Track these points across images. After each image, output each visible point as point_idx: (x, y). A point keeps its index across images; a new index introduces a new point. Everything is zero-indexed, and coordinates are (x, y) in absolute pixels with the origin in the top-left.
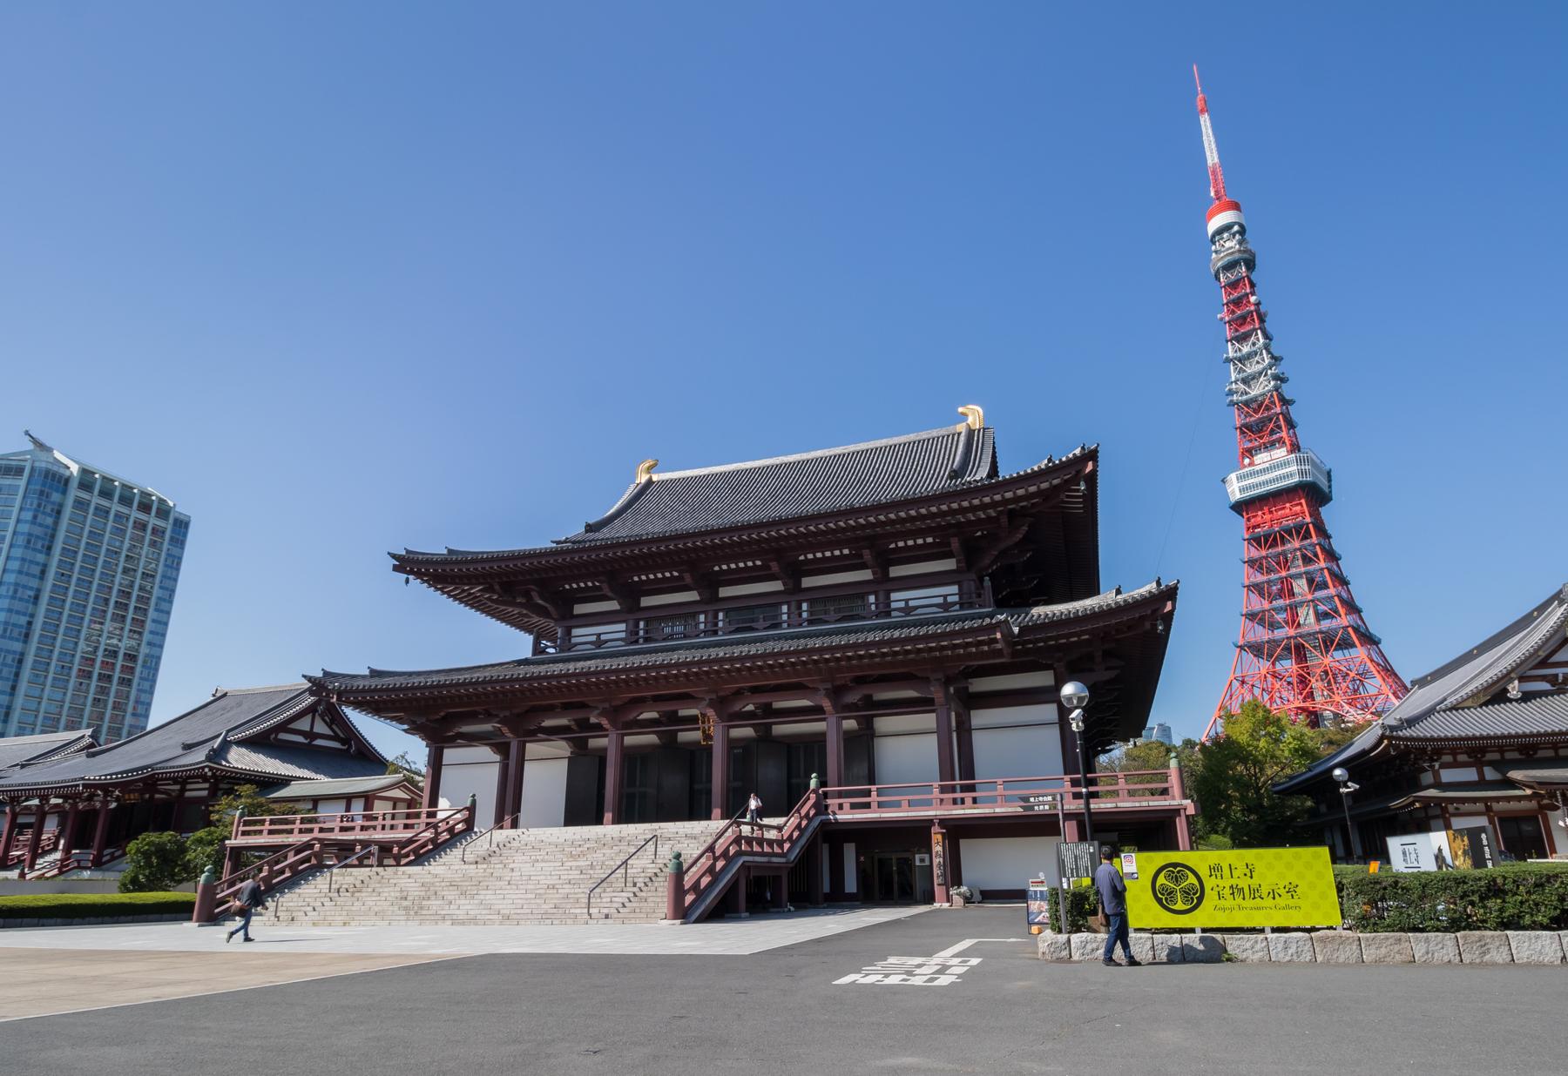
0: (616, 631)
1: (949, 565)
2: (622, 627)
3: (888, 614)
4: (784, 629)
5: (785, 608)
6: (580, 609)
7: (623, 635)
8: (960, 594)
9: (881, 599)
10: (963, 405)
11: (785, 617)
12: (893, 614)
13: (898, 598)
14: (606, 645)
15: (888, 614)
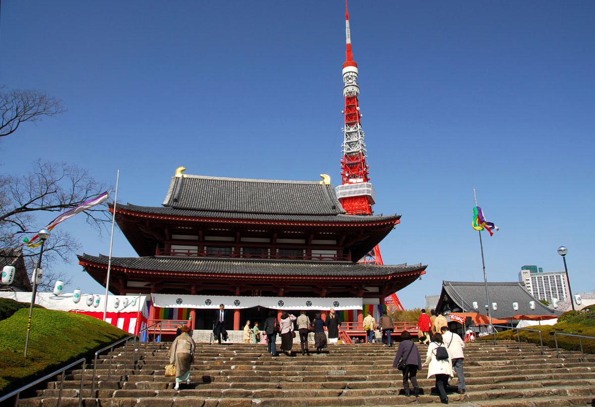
0: (194, 249)
1: (333, 242)
2: (196, 248)
3: (310, 259)
6: (175, 237)
11: (269, 254)
12: (313, 259)
13: (315, 253)
15: (310, 259)
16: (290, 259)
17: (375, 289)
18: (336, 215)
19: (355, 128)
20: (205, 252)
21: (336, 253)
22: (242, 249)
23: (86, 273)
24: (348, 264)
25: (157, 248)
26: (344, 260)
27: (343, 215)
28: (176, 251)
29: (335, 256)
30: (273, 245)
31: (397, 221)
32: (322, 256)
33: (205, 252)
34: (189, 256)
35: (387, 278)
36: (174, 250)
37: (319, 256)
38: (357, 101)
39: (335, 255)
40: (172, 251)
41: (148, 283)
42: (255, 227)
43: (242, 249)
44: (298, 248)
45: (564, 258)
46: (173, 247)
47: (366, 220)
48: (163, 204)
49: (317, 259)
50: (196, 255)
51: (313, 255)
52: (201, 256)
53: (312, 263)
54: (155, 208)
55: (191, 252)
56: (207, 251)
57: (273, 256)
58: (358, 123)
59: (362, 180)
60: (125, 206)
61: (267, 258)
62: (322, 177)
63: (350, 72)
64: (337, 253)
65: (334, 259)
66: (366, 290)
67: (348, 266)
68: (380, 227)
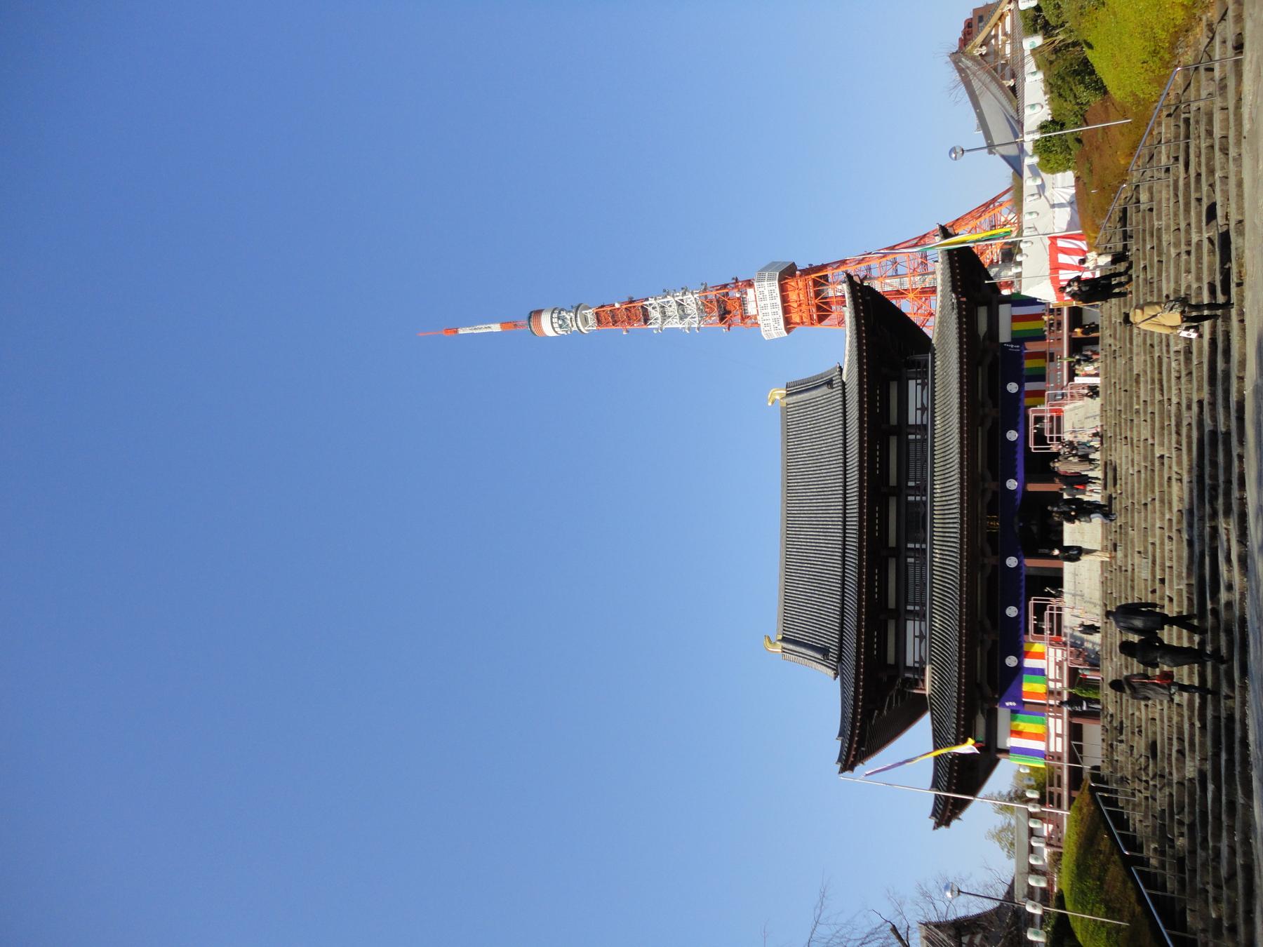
0: (912, 628)
2: (910, 624)
3: (925, 427)
5: (911, 498)
6: (891, 659)
8: (916, 379)
9: (913, 431)
10: (767, 401)
11: (918, 498)
12: (924, 423)
13: (913, 417)
14: (924, 632)
16: (926, 461)
17: (983, 313)
18: (844, 384)
19: (653, 308)
20: (917, 608)
21: (915, 381)
22: (910, 546)
23: (960, 817)
24: (933, 362)
25: (915, 691)
26: (926, 366)
27: (845, 372)
28: (917, 659)
31: (856, 279)
32: (919, 406)
33: (917, 608)
34: (925, 637)
35: (964, 303)
36: (915, 662)
37: (919, 412)
38: (603, 306)
39: (917, 384)
40: (917, 665)
41: (980, 712)
43: (910, 546)
44: (904, 446)
46: (910, 662)
48: (833, 676)
50: (923, 623)
52: (924, 616)
53: (933, 425)
54: (843, 693)
56: (915, 604)
57: (921, 490)
58: (645, 303)
59: (750, 291)
61: (926, 501)
62: (773, 403)
64: (912, 379)
65: (924, 385)
66: (984, 336)
67: (938, 363)
68: (865, 303)
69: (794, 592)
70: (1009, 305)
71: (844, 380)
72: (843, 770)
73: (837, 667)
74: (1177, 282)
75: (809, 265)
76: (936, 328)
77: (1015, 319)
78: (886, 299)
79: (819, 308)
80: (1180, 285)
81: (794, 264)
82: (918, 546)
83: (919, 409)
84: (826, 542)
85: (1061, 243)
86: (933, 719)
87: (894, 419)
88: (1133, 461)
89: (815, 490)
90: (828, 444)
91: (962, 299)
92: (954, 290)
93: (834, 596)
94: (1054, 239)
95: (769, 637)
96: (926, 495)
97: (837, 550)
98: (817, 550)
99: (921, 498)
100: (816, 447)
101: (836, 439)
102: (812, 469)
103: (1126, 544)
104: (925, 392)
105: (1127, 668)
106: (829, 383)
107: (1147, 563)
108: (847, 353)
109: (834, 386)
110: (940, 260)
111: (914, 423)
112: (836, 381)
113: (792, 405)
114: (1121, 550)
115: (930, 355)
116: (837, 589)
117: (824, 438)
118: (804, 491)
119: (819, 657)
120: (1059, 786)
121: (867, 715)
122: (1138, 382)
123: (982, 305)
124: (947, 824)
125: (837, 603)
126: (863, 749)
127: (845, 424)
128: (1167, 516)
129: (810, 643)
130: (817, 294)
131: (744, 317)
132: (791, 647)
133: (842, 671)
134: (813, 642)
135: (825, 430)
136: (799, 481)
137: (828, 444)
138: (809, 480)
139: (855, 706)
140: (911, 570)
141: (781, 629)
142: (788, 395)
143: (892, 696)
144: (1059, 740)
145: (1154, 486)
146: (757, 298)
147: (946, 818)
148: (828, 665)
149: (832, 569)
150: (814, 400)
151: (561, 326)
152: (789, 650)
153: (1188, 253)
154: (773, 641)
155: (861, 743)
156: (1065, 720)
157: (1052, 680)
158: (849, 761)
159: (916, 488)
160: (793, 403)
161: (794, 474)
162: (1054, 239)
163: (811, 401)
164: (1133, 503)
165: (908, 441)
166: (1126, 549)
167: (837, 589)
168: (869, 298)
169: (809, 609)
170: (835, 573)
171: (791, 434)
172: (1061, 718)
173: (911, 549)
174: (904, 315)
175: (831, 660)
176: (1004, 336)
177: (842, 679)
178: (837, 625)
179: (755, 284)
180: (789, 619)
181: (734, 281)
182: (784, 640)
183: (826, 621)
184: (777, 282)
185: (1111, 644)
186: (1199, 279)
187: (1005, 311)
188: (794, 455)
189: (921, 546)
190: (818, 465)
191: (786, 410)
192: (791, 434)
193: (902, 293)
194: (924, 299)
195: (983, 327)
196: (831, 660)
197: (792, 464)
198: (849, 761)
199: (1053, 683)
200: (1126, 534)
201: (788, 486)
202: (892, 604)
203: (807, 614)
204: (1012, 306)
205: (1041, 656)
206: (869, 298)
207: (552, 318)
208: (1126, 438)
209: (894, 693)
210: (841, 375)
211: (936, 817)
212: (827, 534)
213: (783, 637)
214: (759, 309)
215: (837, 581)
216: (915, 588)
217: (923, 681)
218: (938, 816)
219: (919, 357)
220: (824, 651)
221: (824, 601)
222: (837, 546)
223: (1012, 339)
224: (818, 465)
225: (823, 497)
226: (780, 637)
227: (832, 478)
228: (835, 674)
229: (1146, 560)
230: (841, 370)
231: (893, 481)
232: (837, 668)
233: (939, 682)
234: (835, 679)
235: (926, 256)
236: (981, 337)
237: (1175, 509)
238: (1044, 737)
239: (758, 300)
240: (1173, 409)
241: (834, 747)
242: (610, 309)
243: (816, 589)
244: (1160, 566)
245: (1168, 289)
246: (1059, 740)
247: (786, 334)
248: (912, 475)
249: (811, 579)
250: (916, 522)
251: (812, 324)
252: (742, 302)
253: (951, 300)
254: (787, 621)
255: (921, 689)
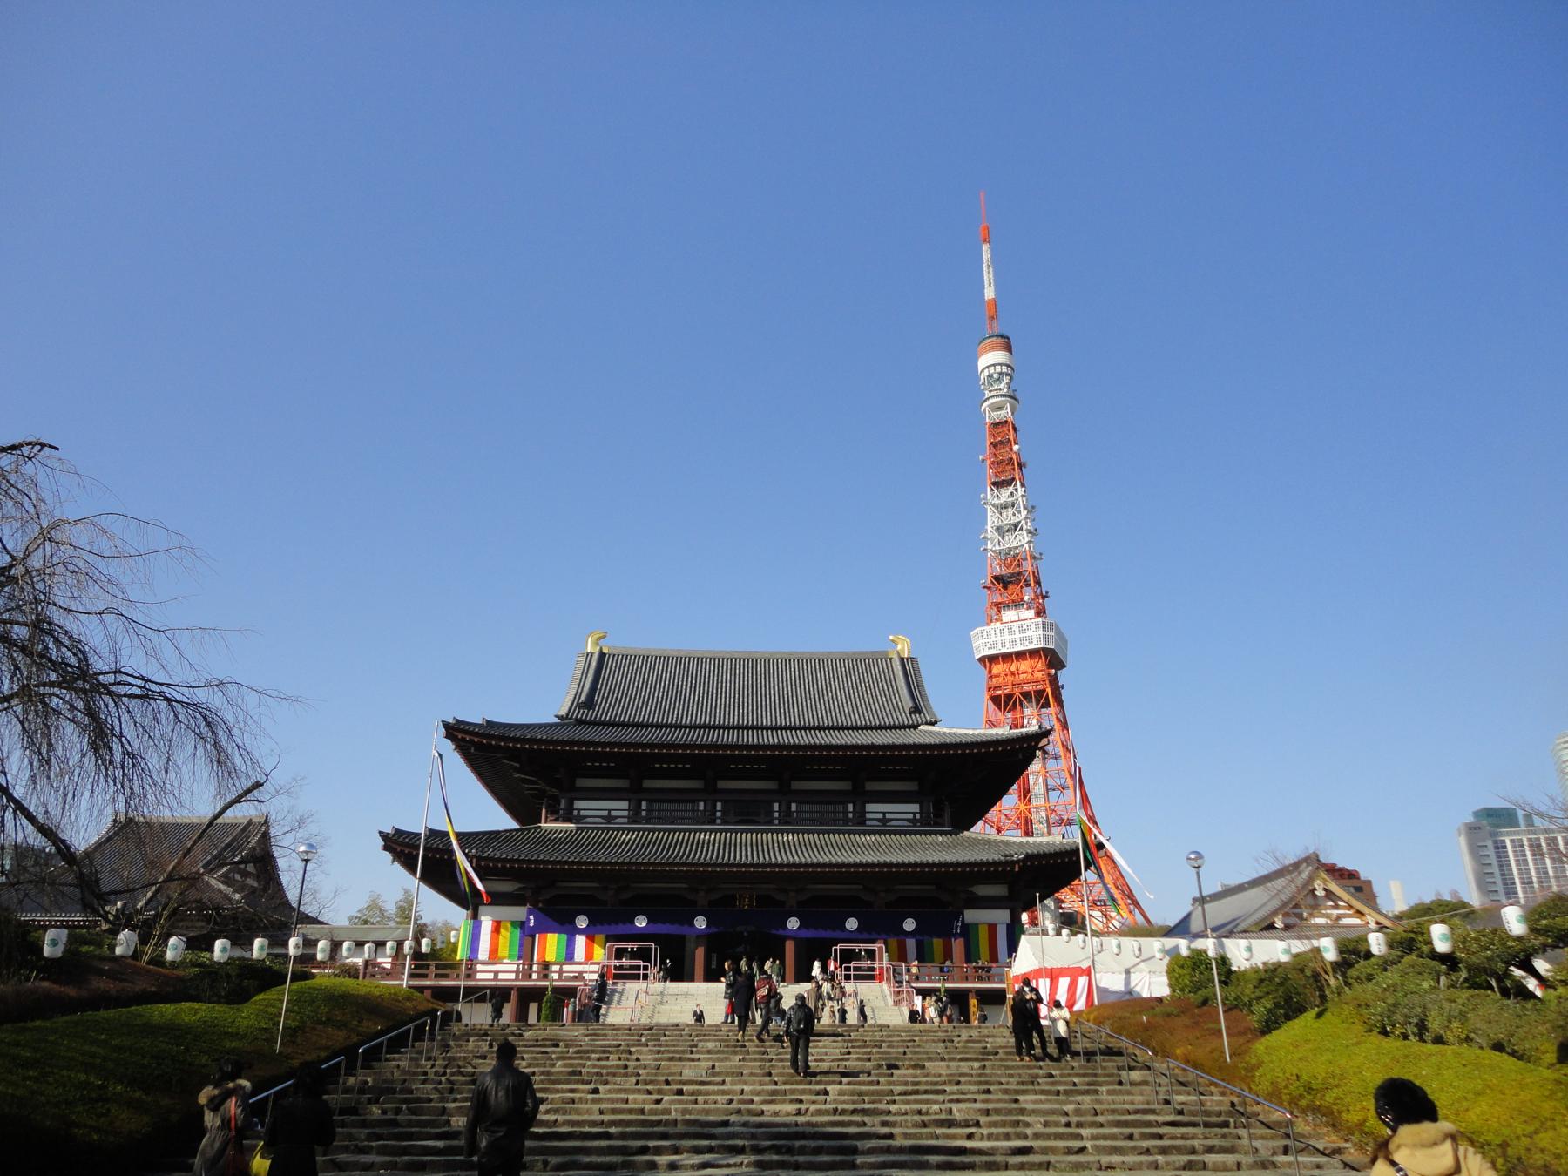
0: (620, 807)
2: (624, 805)
3: (864, 824)
4: (776, 825)
5: (776, 806)
6: (582, 782)
7: (626, 813)
8: (921, 813)
9: (858, 809)
11: (776, 815)
12: (867, 822)
13: (874, 809)
17: (999, 890)
18: (915, 727)
19: (1012, 493)
20: (644, 813)
22: (719, 806)
23: (396, 863)
24: (941, 833)
25: (544, 810)
26: (936, 824)
27: (930, 728)
28: (582, 813)
29: (914, 816)
30: (785, 794)
31: (1044, 742)
33: (644, 813)
34: (609, 823)
35: (1013, 869)
36: (579, 810)
37: (881, 816)
38: (1015, 429)
39: (914, 813)
40: (575, 813)
42: (742, 759)
43: (719, 806)
44: (839, 798)
45: (1198, 874)
46: (579, 804)
47: (979, 740)
48: (560, 714)
49: (878, 824)
50: (626, 820)
51: (868, 816)
52: (635, 822)
53: (865, 833)
54: (540, 726)
55: (613, 813)
56: (648, 810)
57: (786, 818)
58: (1018, 482)
59: (1031, 613)
60: (476, 725)
61: (770, 823)
62: (893, 641)
63: (994, 365)
64: (921, 808)
65: (913, 821)
67: (940, 839)
69: (661, 668)
70: (1009, 921)
71: (921, 727)
72: (446, 725)
73: (571, 718)
74: (1034, 1112)
75: (1063, 686)
76: (983, 836)
77: (992, 928)
78: (1018, 778)
79: (1009, 697)
80: (1030, 1115)
81: (1064, 666)
82: (719, 814)
83: (884, 816)
84: (723, 706)
85: (1082, 981)
86: (511, 831)
87: (871, 786)
88: (821, 1060)
89: (785, 692)
90: (841, 708)
91: (1017, 866)
92: (1028, 857)
93: (656, 715)
94: (1088, 972)
95: (604, 637)
96: (779, 824)
97: (713, 719)
98: (712, 695)
99: (776, 818)
100: (839, 694)
101: (848, 718)
102: (811, 689)
103: (723, 1052)
104: (905, 823)
105: (578, 1052)
106: (916, 710)
107: (702, 1076)
108: (954, 731)
109: (913, 716)
110: (1065, 841)
111: (867, 810)
112: (919, 718)
113: (889, 665)
114: (716, 1046)
115: (950, 829)
116: (665, 719)
117: (849, 703)
118: (785, 679)
119: (583, 698)
120: (436, 976)
121: (514, 754)
122: (915, 1067)
123: (1010, 890)
124: (386, 848)
125: (648, 719)
126: (472, 750)
127: (866, 728)
128: (756, 1099)
129: (599, 687)
130: (1026, 695)
131: (999, 606)
132: (594, 664)
133: (566, 724)
134: (601, 689)
135: (859, 704)
136: (797, 673)
137: (841, 708)
138: (798, 685)
139: (523, 740)
140: (689, 806)
141: (616, 652)
142: (902, 659)
143: (538, 784)
144: (491, 976)
145: (792, 1084)
146: (1022, 622)
147: (394, 846)
148: (573, 708)
149: (690, 712)
150: (896, 691)
151: (990, 376)
152: (590, 661)
153: (1068, 1125)
154: (601, 642)
155: (479, 746)
156: (514, 983)
157: (561, 969)
158: (457, 732)
159: (789, 813)
160: (892, 666)
161: (805, 667)
162: (1088, 972)
163: (895, 688)
164: (771, 1060)
165: (845, 803)
166: (718, 1052)
167: (665, 719)
168: (1020, 757)
169: (640, 686)
170: (685, 716)
171: (855, 663)
172: (517, 979)
173: (715, 808)
174: (1000, 798)
175: (579, 712)
176: (971, 916)
177: (556, 725)
178: (622, 719)
179: (1040, 620)
180: (628, 661)
181: (1044, 594)
182: (602, 655)
183: (626, 706)
184: (1042, 646)
185: (605, 1035)
186: (1037, 1136)
187: (1001, 917)
188: (828, 667)
189: (719, 818)
190: (817, 696)
191: (883, 657)
192: (855, 663)
193: (1025, 797)
194: (1018, 822)
195: (984, 890)
196: (579, 712)
197: (817, 664)
198: (457, 732)
199: (558, 970)
200: (735, 1053)
201: (790, 660)
202: (648, 784)
203: (634, 683)
204: (1008, 925)
205: (589, 957)
206: (1020, 757)
207: (1001, 365)
208: (849, 1053)
209: (541, 785)
210: (927, 723)
211: (393, 835)
212: (732, 707)
213: (604, 655)
214: (1009, 624)
215: (675, 719)
216: (668, 810)
217: (556, 820)
218: (396, 837)
219: (947, 817)
220: (589, 703)
221: (650, 704)
222: (717, 718)
223: (968, 925)
224: (817, 696)
225: (777, 702)
226: (605, 651)
227: (801, 713)
228: (562, 716)
229: (704, 1072)
230: (933, 723)
231: (797, 785)
232: (570, 719)
233: (555, 838)
234: (556, 716)
235: (1070, 824)
236: (970, 889)
237: (764, 1107)
238: (494, 957)
239: (1020, 623)
240: (883, 1106)
241: (474, 716)
242: (1012, 438)
243: (665, 694)
244: (698, 1090)
245: (1026, 1101)
246: (491, 976)
247: (977, 658)
248: (805, 807)
249: (677, 688)
250: (748, 812)
251: (989, 689)
252: (1018, 604)
253: (1016, 854)
254: (624, 659)
255: (546, 818)
